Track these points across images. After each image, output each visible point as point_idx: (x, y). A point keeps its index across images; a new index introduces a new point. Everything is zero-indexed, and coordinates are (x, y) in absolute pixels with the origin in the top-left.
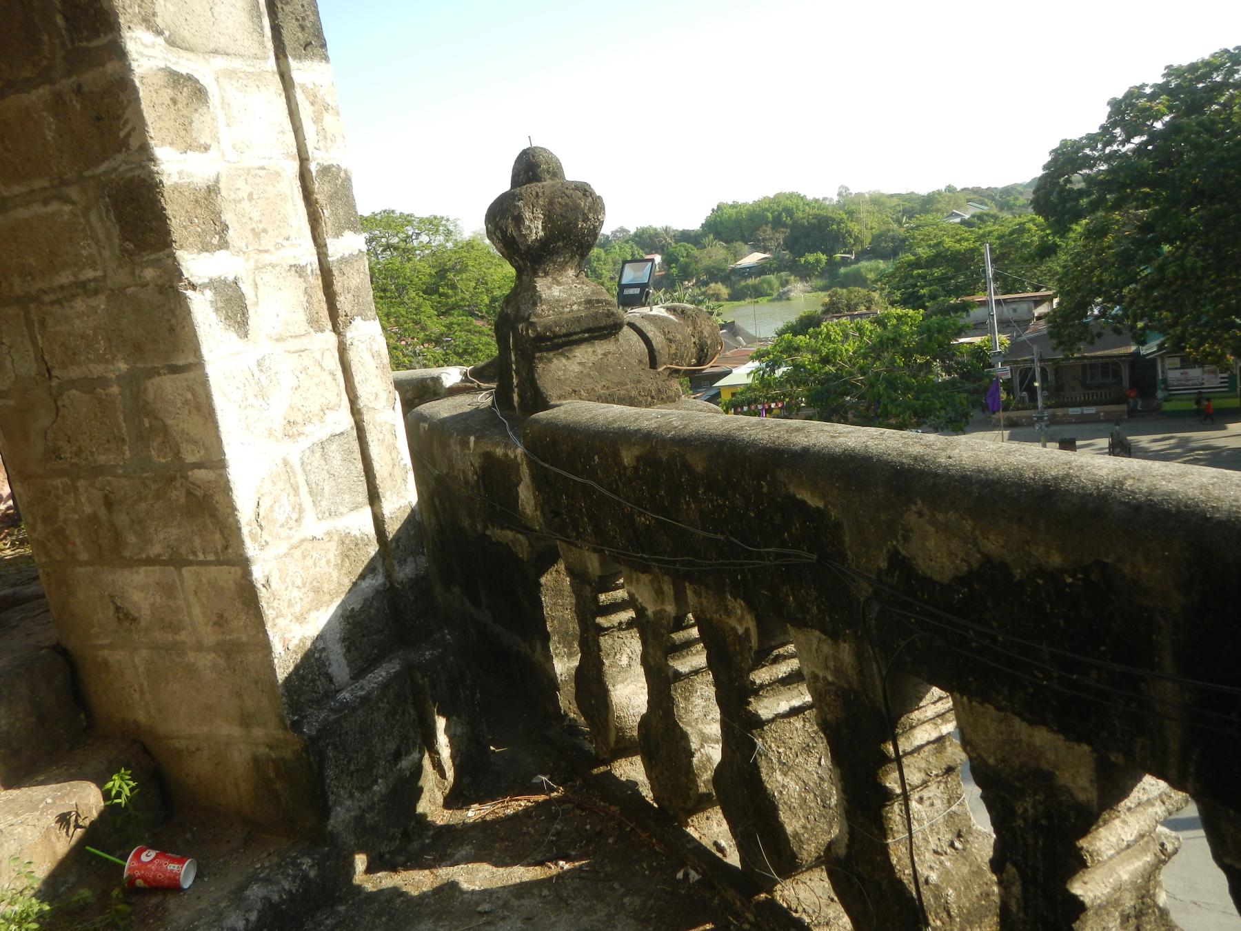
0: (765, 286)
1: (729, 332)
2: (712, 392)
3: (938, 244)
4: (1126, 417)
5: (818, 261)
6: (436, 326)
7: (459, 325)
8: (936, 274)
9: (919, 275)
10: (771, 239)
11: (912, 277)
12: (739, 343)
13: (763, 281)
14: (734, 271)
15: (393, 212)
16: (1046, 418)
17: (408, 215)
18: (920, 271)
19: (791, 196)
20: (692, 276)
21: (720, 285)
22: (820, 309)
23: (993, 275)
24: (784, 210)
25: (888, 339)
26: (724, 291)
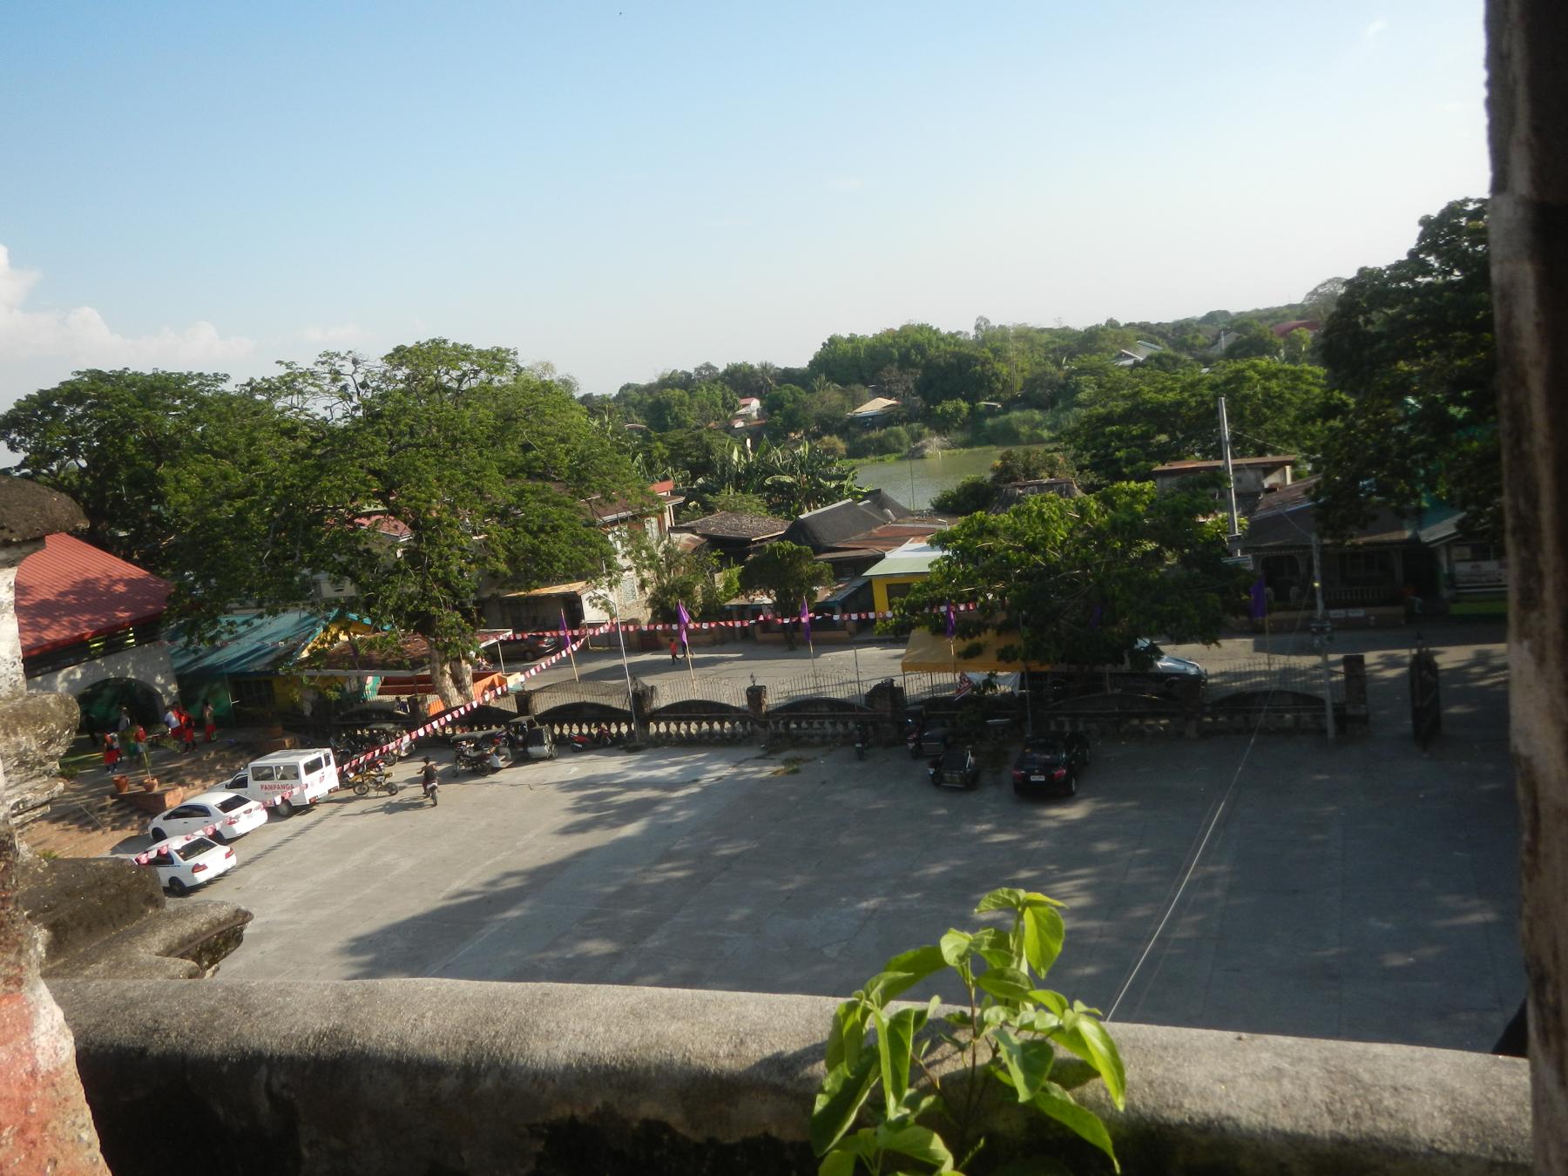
0: (892, 439)
1: (874, 502)
2: (859, 583)
4: (1403, 622)
5: (958, 410)
6: (501, 492)
7: (532, 493)
8: (1134, 433)
9: (1112, 433)
11: (1103, 434)
12: (888, 518)
15: (445, 341)
16: (1328, 629)
17: (464, 347)
18: (1114, 428)
19: (921, 328)
20: (800, 426)
21: (835, 439)
22: (989, 476)
23: (1230, 437)
25: (1124, 523)
26: (841, 446)
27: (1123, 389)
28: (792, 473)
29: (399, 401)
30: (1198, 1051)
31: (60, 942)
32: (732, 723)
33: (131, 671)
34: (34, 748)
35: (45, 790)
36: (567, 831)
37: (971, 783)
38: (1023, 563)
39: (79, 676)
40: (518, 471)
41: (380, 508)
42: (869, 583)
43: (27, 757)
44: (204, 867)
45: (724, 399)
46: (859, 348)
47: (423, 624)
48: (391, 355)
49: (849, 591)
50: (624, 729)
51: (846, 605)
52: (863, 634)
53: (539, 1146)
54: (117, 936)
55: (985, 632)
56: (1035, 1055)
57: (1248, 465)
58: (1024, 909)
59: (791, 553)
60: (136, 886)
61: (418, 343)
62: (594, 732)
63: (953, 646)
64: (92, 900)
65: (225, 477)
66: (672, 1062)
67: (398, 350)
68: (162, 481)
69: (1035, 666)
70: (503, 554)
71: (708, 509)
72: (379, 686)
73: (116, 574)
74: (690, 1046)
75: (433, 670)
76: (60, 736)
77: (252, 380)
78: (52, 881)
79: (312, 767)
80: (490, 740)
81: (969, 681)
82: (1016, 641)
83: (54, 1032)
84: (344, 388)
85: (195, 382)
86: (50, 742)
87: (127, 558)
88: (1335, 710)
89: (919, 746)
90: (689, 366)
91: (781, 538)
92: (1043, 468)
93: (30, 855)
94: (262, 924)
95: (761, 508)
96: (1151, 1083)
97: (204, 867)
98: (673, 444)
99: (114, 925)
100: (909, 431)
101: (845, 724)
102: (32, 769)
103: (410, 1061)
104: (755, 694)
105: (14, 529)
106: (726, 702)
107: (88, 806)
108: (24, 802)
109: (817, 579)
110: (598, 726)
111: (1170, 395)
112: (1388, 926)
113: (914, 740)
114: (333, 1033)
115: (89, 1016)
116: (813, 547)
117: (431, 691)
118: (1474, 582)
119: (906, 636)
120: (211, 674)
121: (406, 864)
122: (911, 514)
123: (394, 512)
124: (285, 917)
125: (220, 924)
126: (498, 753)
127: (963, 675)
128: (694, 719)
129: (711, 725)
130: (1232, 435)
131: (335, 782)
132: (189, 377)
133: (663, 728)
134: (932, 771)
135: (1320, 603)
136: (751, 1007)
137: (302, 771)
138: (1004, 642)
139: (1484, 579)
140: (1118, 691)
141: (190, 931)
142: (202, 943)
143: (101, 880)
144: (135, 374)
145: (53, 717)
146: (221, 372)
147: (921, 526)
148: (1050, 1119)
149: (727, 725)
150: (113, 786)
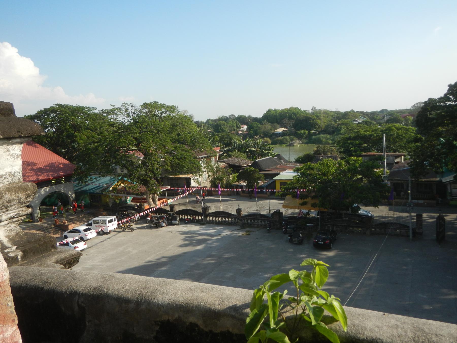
0: (285, 140)
2: (272, 181)
3: (358, 132)
5: (305, 133)
6: (170, 147)
7: (179, 147)
8: (357, 143)
9: (350, 143)
10: (287, 123)
11: (348, 143)
12: (281, 162)
15: (158, 102)
17: (163, 104)
18: (351, 141)
19: (296, 108)
20: (258, 134)
21: (268, 139)
22: (312, 153)
23: (386, 146)
24: (293, 113)
25: (352, 169)
26: (270, 141)
27: (354, 130)
28: (255, 147)
29: (144, 118)
30: (370, 317)
31: (25, 256)
32: (232, 219)
33: (62, 190)
34: (23, 198)
35: (25, 211)
36: (182, 246)
37: (301, 242)
38: (321, 178)
39: (48, 190)
40: (176, 141)
41: (136, 149)
42: (275, 181)
43: (21, 201)
44: (78, 247)
45: (237, 125)
47: (145, 183)
48: (142, 105)
49: (269, 183)
50: (200, 218)
51: (267, 187)
52: (272, 196)
53: (157, 328)
54: (42, 256)
55: (308, 198)
56: (318, 311)
57: (391, 155)
58: (316, 266)
59: (253, 171)
60: (49, 242)
61: (150, 102)
62: (191, 218)
63: (298, 201)
64: (36, 245)
65: (93, 137)
66: (201, 305)
67: (145, 104)
68: (76, 136)
69: (322, 209)
70: (169, 164)
71: (230, 156)
72: (131, 200)
73: (60, 162)
74: (207, 301)
75: (147, 196)
76: (31, 195)
77: (103, 109)
78: (25, 238)
79: (110, 221)
80: (161, 218)
81: (302, 212)
82: (317, 201)
83: (3, 270)
84: (129, 113)
85: (87, 109)
86: (28, 197)
87: (64, 158)
88: (413, 230)
89: (286, 230)
90: (227, 114)
91: (250, 166)
92: (329, 151)
93: (20, 230)
94: (92, 265)
95: (245, 157)
96: (354, 326)
97: (78, 247)
98: (221, 137)
99: (42, 253)
101: (265, 222)
102: (22, 204)
103: (120, 298)
104: (239, 211)
105: (23, 132)
106: (230, 212)
107: (47, 227)
108: (19, 214)
109: (259, 179)
110: (193, 216)
111: (368, 132)
112: (425, 297)
113: (285, 228)
114: (98, 288)
115: (29, 277)
116: (259, 169)
117: (146, 202)
119: (284, 197)
120: (84, 192)
121: (135, 252)
122: (289, 162)
123: (140, 150)
124: (99, 264)
125: (73, 256)
126: (163, 222)
127: (300, 210)
128: (220, 217)
129: (225, 219)
130: (387, 146)
131: (116, 226)
132: (86, 108)
133: (211, 218)
134: (289, 238)
135: (410, 197)
136: (227, 291)
138: (313, 201)
140: (347, 219)
141: (64, 257)
142: (67, 261)
143: (39, 239)
145: (30, 189)
146: (94, 107)
147: (292, 166)
148: (320, 334)
149: (230, 219)
150: (55, 222)
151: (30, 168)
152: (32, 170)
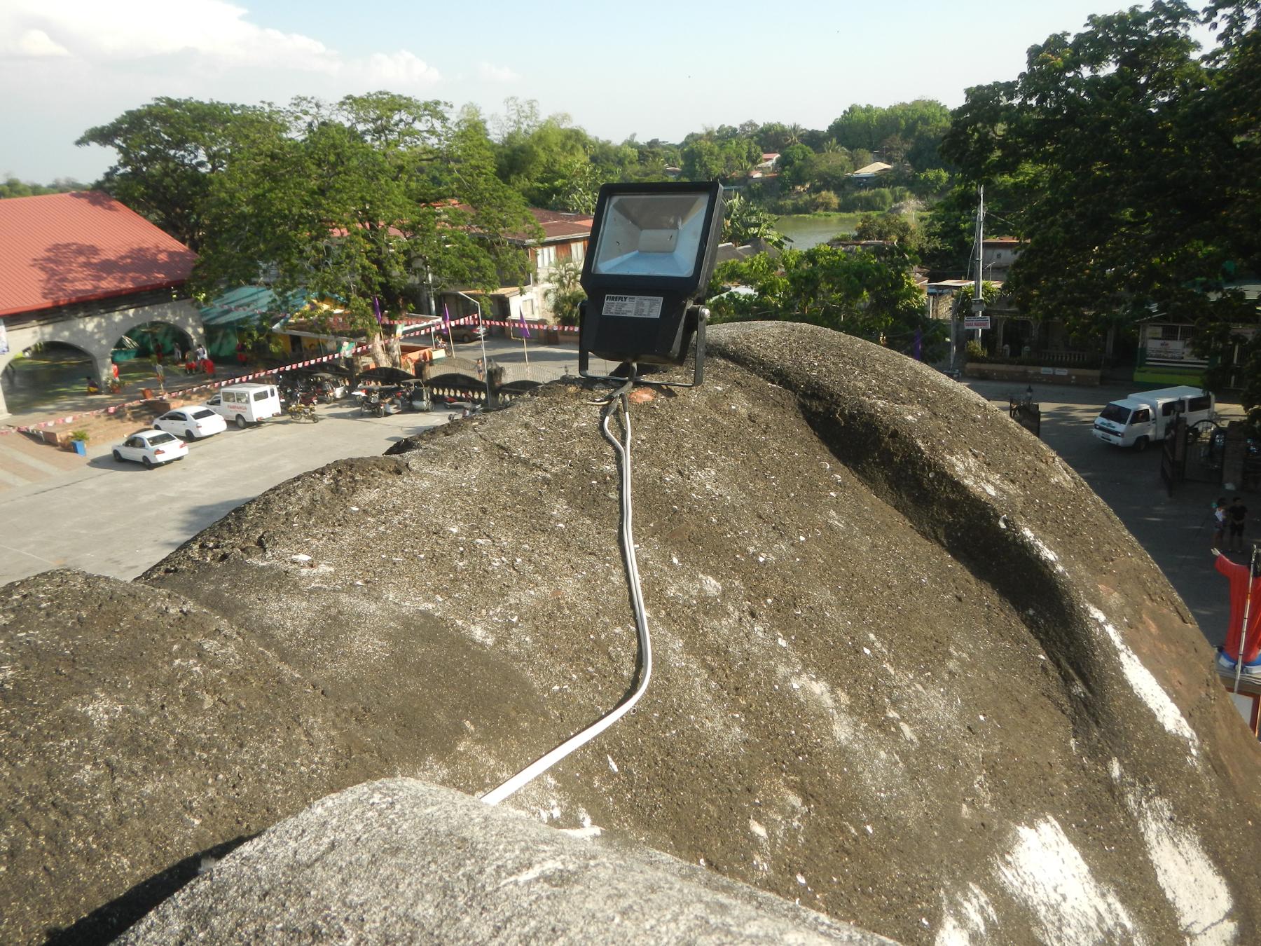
0: (878, 199)
1: (753, 247)
5: (939, 178)
10: (898, 149)
13: (877, 195)
14: (849, 179)
19: (930, 104)
20: (806, 181)
26: (833, 198)
44: (163, 452)
45: (749, 152)
46: (871, 117)
67: (348, 98)
73: (162, 247)
79: (259, 397)
90: (735, 121)
97: (163, 452)
100: (893, 193)
118: (1164, 357)
126: (392, 403)
132: (233, 106)
137: (252, 398)
139: (1170, 355)
144: (197, 102)
151: (82, 259)
152: (87, 265)
